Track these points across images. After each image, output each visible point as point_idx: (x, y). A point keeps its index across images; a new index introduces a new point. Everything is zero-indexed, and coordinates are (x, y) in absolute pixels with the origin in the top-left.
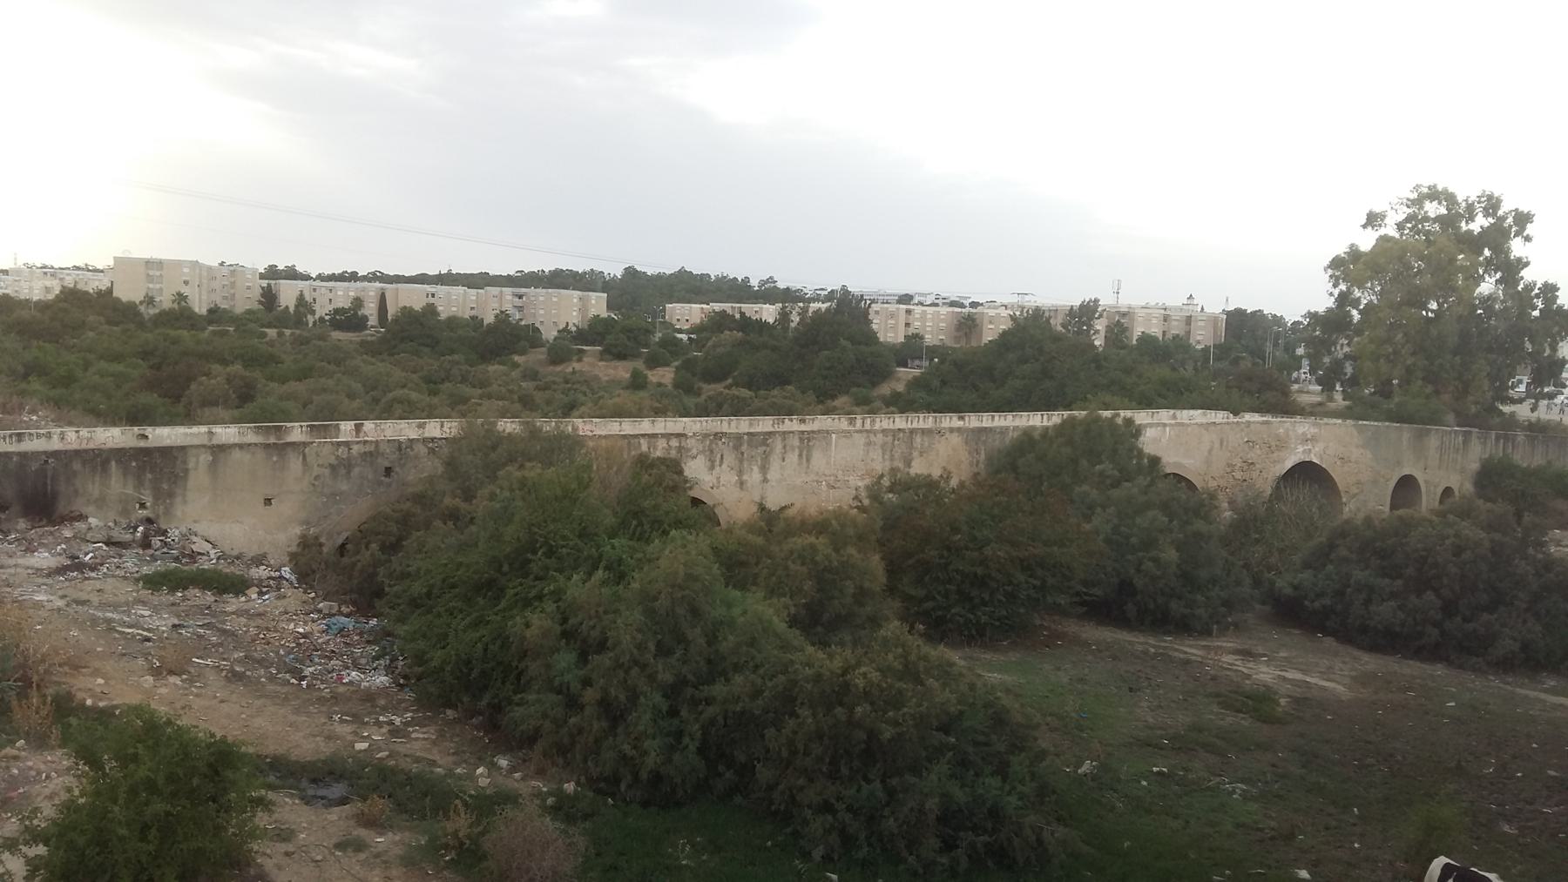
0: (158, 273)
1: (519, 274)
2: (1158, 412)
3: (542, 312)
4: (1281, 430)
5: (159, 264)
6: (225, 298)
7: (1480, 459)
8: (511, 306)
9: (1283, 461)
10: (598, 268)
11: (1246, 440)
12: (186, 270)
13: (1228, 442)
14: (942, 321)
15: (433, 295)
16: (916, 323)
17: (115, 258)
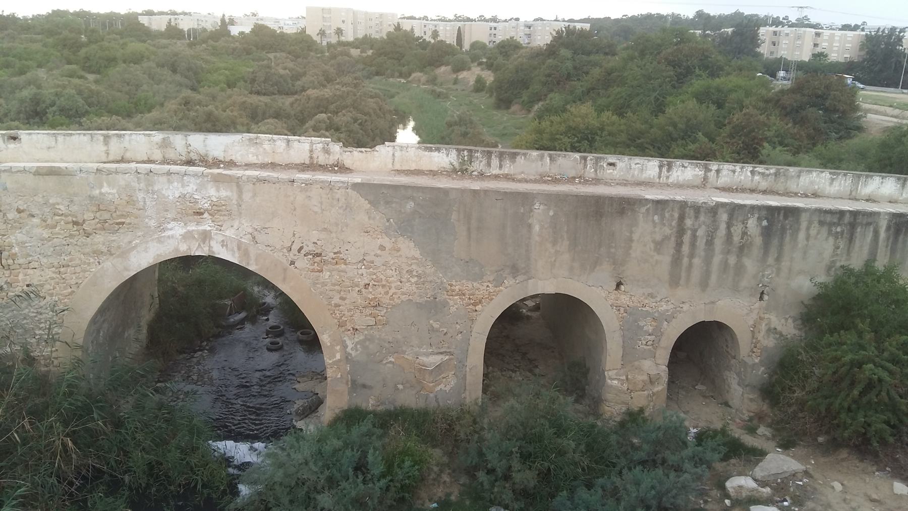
0: (329, 16)
1: (624, 17)
3: (539, 38)
4: (105, 189)
5: (329, 10)
6: (377, 32)
7: (829, 269)
8: (523, 34)
9: (124, 254)
10: (677, 12)
12: (343, 14)
15: (495, 29)
16: (823, 44)
17: (308, 9)
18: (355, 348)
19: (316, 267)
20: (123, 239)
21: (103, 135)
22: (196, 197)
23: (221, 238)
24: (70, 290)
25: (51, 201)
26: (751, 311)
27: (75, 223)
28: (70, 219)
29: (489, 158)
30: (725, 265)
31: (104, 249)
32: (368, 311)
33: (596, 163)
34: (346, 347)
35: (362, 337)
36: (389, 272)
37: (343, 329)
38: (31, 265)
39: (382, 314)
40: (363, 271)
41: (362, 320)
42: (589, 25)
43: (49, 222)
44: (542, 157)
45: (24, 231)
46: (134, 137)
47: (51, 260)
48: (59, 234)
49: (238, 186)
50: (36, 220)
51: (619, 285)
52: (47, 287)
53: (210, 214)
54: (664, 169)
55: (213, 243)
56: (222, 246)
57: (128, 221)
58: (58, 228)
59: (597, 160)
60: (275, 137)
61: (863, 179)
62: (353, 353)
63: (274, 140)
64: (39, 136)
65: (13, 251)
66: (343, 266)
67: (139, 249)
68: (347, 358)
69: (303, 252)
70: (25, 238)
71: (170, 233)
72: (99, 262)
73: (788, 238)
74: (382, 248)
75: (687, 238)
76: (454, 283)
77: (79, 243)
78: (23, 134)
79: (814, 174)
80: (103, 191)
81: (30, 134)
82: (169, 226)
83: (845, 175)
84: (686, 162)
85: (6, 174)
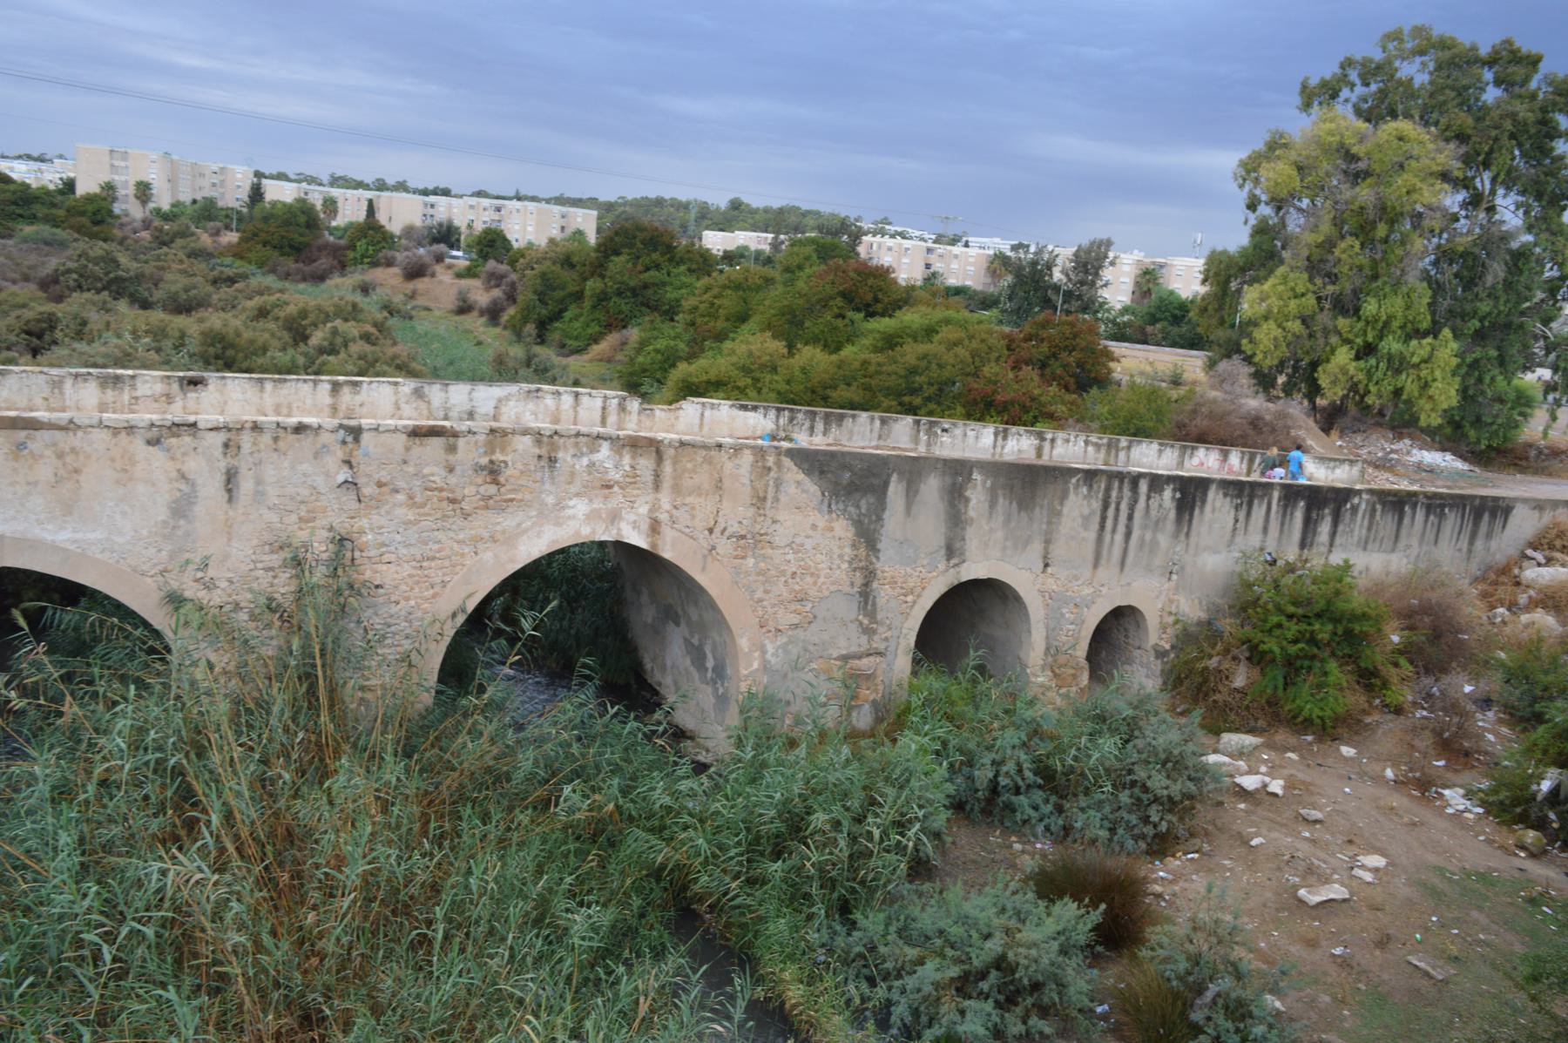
2: (356, 384)
3: (517, 227)
9: (510, 539)
11: (341, 478)
13: (259, 481)
14: (971, 264)
18: (775, 655)
19: (739, 552)
20: (507, 521)
21: (329, 381)
22: (607, 465)
23: (632, 517)
24: (431, 592)
25: (426, 471)
26: (1160, 592)
27: (453, 501)
28: (445, 494)
29: (813, 420)
30: (1142, 540)
31: (486, 535)
32: (793, 607)
33: (930, 428)
34: (764, 652)
35: (785, 639)
36: (819, 557)
37: (764, 630)
38: (386, 558)
39: (808, 609)
40: (790, 557)
41: (786, 618)
42: (595, 213)
43: (418, 499)
44: (872, 419)
45: (382, 512)
46: (374, 386)
47: (413, 550)
48: (430, 515)
49: (658, 452)
50: (401, 497)
51: (1046, 565)
52: (403, 587)
53: (621, 488)
54: (1000, 438)
55: (623, 525)
56: (634, 528)
57: (519, 496)
58: (426, 510)
59: (932, 424)
60: (561, 389)
61: (1189, 452)
62: (773, 660)
63: (558, 393)
64: (237, 381)
65: (364, 539)
66: (770, 551)
67: (530, 534)
68: (765, 667)
69: (727, 533)
70: (383, 521)
71: (569, 512)
72: (476, 553)
73: (1197, 511)
74: (814, 527)
75: (1111, 512)
76: (886, 569)
77: (454, 527)
78: (212, 376)
79: (1144, 445)
80: (494, 458)
81: (224, 378)
82: (571, 503)
83: (1172, 446)
84: (1022, 429)
85: (373, 434)
